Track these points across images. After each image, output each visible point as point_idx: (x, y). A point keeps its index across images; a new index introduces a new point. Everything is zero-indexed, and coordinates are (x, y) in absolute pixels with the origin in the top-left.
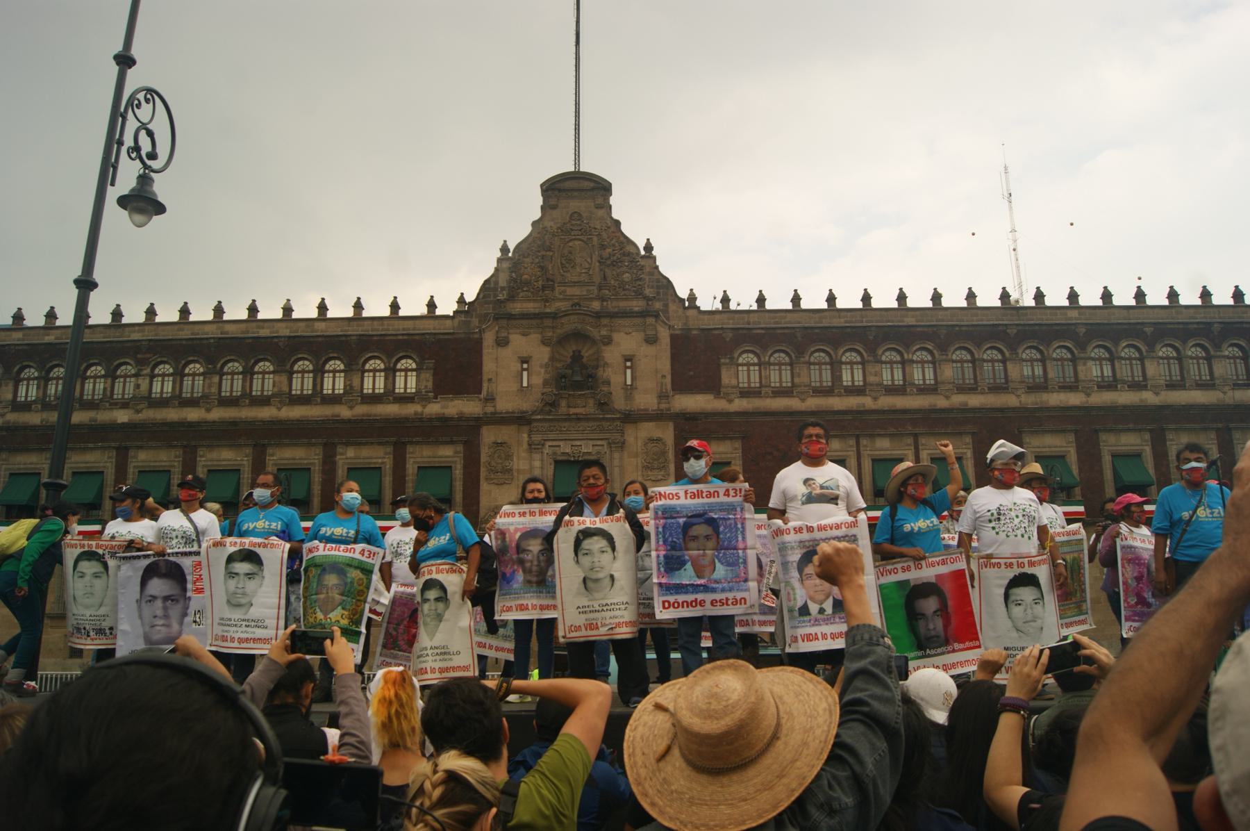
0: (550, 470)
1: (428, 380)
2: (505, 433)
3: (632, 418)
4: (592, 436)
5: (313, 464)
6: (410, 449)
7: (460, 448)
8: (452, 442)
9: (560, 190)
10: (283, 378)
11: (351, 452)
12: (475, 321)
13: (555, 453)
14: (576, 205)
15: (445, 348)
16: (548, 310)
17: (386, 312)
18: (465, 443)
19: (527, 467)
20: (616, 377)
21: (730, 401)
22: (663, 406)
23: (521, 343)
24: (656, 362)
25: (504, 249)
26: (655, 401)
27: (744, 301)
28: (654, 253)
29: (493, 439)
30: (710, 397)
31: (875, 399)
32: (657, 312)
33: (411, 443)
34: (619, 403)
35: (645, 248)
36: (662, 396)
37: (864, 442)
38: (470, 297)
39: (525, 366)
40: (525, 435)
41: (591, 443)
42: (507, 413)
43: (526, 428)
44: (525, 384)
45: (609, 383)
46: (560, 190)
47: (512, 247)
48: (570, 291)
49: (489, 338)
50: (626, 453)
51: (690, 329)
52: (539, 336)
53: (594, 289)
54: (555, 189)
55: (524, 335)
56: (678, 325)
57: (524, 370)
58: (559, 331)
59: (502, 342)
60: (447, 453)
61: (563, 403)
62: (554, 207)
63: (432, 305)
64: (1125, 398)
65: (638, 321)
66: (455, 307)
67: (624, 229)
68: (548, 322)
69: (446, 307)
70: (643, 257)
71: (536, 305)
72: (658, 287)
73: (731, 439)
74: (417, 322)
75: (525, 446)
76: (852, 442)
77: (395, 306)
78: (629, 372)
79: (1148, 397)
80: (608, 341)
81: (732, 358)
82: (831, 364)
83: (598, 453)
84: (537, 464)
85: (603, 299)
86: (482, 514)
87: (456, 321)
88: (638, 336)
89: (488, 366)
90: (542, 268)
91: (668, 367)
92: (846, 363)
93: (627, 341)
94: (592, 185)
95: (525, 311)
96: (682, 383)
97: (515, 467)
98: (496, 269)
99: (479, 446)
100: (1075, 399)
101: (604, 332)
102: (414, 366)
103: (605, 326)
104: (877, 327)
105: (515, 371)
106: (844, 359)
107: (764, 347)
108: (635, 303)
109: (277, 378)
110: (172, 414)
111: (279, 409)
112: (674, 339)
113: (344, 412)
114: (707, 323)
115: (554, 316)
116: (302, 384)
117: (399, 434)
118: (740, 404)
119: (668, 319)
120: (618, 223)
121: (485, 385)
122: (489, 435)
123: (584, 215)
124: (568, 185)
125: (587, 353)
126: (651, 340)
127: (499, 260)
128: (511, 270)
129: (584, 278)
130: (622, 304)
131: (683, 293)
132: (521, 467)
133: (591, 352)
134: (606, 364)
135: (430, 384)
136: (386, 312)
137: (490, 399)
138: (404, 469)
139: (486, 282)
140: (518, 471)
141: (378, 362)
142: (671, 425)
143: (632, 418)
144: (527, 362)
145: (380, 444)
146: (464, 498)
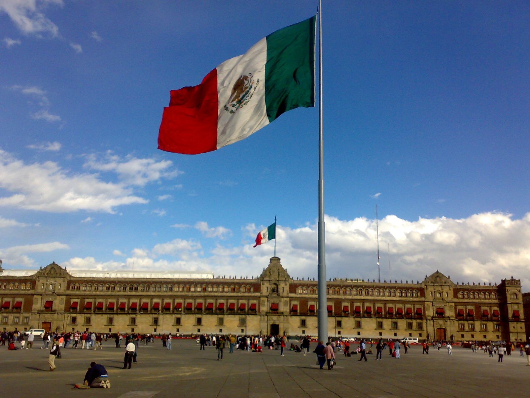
1: (252, 290)
3: (283, 297)
14: (276, 262)
15: (255, 286)
20: (281, 291)
24: (287, 288)
34: (281, 295)
36: (288, 294)
38: (259, 277)
56: (290, 282)
60: (255, 302)
64: (358, 297)
79: (362, 297)
89: (262, 288)
93: (282, 285)
100: (350, 297)
105: (265, 288)
110: (213, 294)
113: (239, 294)
114: (295, 282)
117: (248, 298)
118: (299, 296)
122: (262, 299)
126: (286, 285)
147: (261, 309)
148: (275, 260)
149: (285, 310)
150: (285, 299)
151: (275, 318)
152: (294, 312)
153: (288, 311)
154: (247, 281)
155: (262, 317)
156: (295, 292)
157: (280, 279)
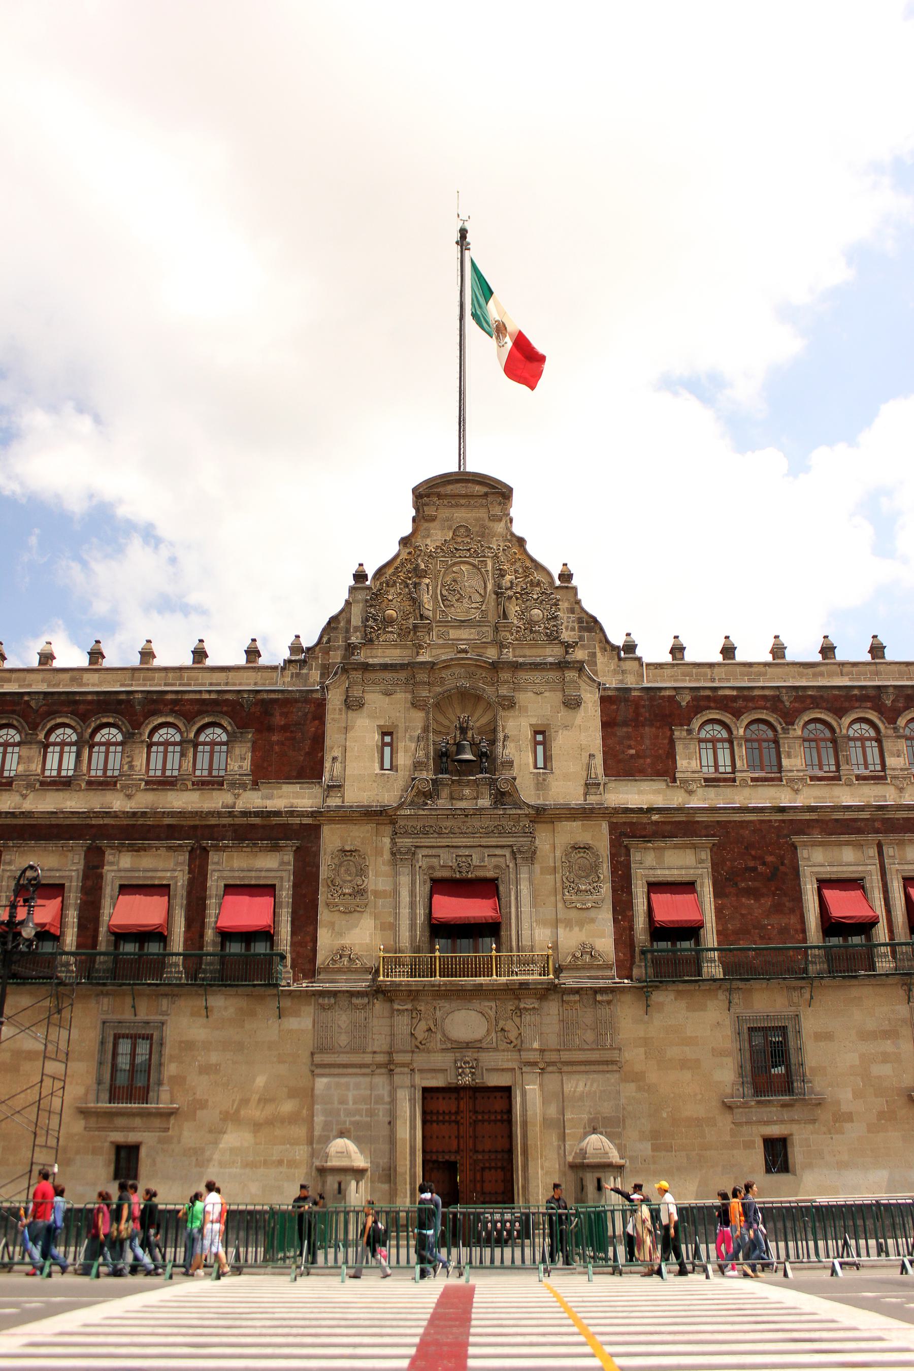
0: (422, 890)
2: (357, 835)
4: (485, 841)
5: (70, 878)
6: (213, 857)
7: (289, 857)
8: (276, 848)
9: (439, 496)
10: (34, 752)
11: (126, 861)
12: (315, 675)
13: (432, 868)
14: (461, 515)
16: (421, 659)
17: (187, 660)
18: (297, 851)
19: (388, 888)
21: (690, 793)
22: (593, 799)
23: (384, 705)
25: (360, 576)
26: (581, 790)
27: (703, 650)
28: (574, 582)
29: (338, 844)
30: (662, 785)
31: (901, 790)
32: (581, 662)
33: (217, 848)
34: (528, 794)
35: (561, 576)
36: (590, 786)
37: (888, 851)
38: (308, 641)
39: (387, 739)
40: (387, 840)
41: (487, 852)
42: (357, 807)
43: (388, 829)
44: (387, 765)
45: (510, 764)
46: (439, 496)
47: (370, 573)
48: (453, 634)
49: (334, 699)
50: (537, 867)
51: (629, 690)
52: (409, 696)
53: (488, 631)
54: (430, 495)
55: (388, 694)
56: (612, 682)
57: (384, 744)
58: (439, 689)
59: (352, 704)
61: (445, 793)
62: (433, 519)
63: (253, 653)
65: (552, 675)
66: (286, 655)
67: (530, 548)
68: (422, 676)
69: (275, 653)
70: (557, 588)
71: (407, 652)
72: (581, 629)
73: (694, 847)
74: (231, 674)
75: (387, 855)
76: (873, 852)
77: (200, 654)
78: (540, 749)
80: (510, 704)
81: (689, 732)
82: (834, 741)
83: (497, 867)
84: (404, 880)
85: (501, 646)
86: (321, 957)
87: (288, 673)
88: (553, 698)
90: (413, 600)
91: (599, 742)
92: (854, 739)
93: (535, 705)
94: (485, 489)
95: (388, 661)
96: (620, 764)
97: (371, 887)
98: (348, 603)
99: (317, 854)
101: (504, 691)
102: (224, 738)
103: (507, 682)
104: (895, 687)
106: (851, 733)
107: (737, 714)
108: (548, 651)
109: (25, 751)
111: (24, 797)
112: (605, 701)
113: (117, 803)
115: (431, 666)
116: (61, 762)
117: (198, 837)
119: (596, 673)
120: (521, 542)
121: (327, 764)
122: (331, 839)
123: (474, 530)
124: (449, 489)
125: (478, 720)
127: (352, 590)
128: (369, 604)
129: (476, 615)
130: (527, 652)
131: (617, 639)
132: (381, 887)
133: (484, 720)
134: (506, 738)
135: (247, 765)
136: (187, 660)
137: (336, 787)
138: (204, 888)
139: (333, 620)
140: (376, 893)
141: (172, 731)
142: (605, 826)
143: (542, 815)
144: (390, 734)
145: (169, 848)
146: (294, 933)
147: (326, 941)
148: (454, 500)
149: (570, 940)
150: (572, 832)
151: (466, 1023)
152: (663, 956)
153: (605, 943)
154: (204, 685)
155: (342, 1019)
156: (664, 768)
157: (509, 655)
